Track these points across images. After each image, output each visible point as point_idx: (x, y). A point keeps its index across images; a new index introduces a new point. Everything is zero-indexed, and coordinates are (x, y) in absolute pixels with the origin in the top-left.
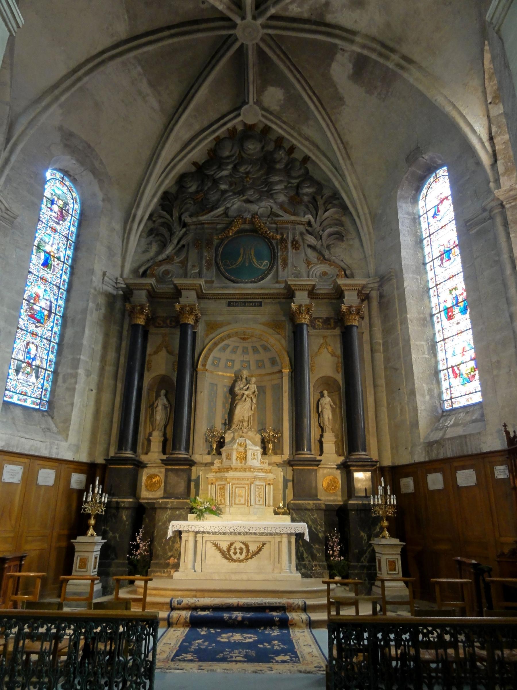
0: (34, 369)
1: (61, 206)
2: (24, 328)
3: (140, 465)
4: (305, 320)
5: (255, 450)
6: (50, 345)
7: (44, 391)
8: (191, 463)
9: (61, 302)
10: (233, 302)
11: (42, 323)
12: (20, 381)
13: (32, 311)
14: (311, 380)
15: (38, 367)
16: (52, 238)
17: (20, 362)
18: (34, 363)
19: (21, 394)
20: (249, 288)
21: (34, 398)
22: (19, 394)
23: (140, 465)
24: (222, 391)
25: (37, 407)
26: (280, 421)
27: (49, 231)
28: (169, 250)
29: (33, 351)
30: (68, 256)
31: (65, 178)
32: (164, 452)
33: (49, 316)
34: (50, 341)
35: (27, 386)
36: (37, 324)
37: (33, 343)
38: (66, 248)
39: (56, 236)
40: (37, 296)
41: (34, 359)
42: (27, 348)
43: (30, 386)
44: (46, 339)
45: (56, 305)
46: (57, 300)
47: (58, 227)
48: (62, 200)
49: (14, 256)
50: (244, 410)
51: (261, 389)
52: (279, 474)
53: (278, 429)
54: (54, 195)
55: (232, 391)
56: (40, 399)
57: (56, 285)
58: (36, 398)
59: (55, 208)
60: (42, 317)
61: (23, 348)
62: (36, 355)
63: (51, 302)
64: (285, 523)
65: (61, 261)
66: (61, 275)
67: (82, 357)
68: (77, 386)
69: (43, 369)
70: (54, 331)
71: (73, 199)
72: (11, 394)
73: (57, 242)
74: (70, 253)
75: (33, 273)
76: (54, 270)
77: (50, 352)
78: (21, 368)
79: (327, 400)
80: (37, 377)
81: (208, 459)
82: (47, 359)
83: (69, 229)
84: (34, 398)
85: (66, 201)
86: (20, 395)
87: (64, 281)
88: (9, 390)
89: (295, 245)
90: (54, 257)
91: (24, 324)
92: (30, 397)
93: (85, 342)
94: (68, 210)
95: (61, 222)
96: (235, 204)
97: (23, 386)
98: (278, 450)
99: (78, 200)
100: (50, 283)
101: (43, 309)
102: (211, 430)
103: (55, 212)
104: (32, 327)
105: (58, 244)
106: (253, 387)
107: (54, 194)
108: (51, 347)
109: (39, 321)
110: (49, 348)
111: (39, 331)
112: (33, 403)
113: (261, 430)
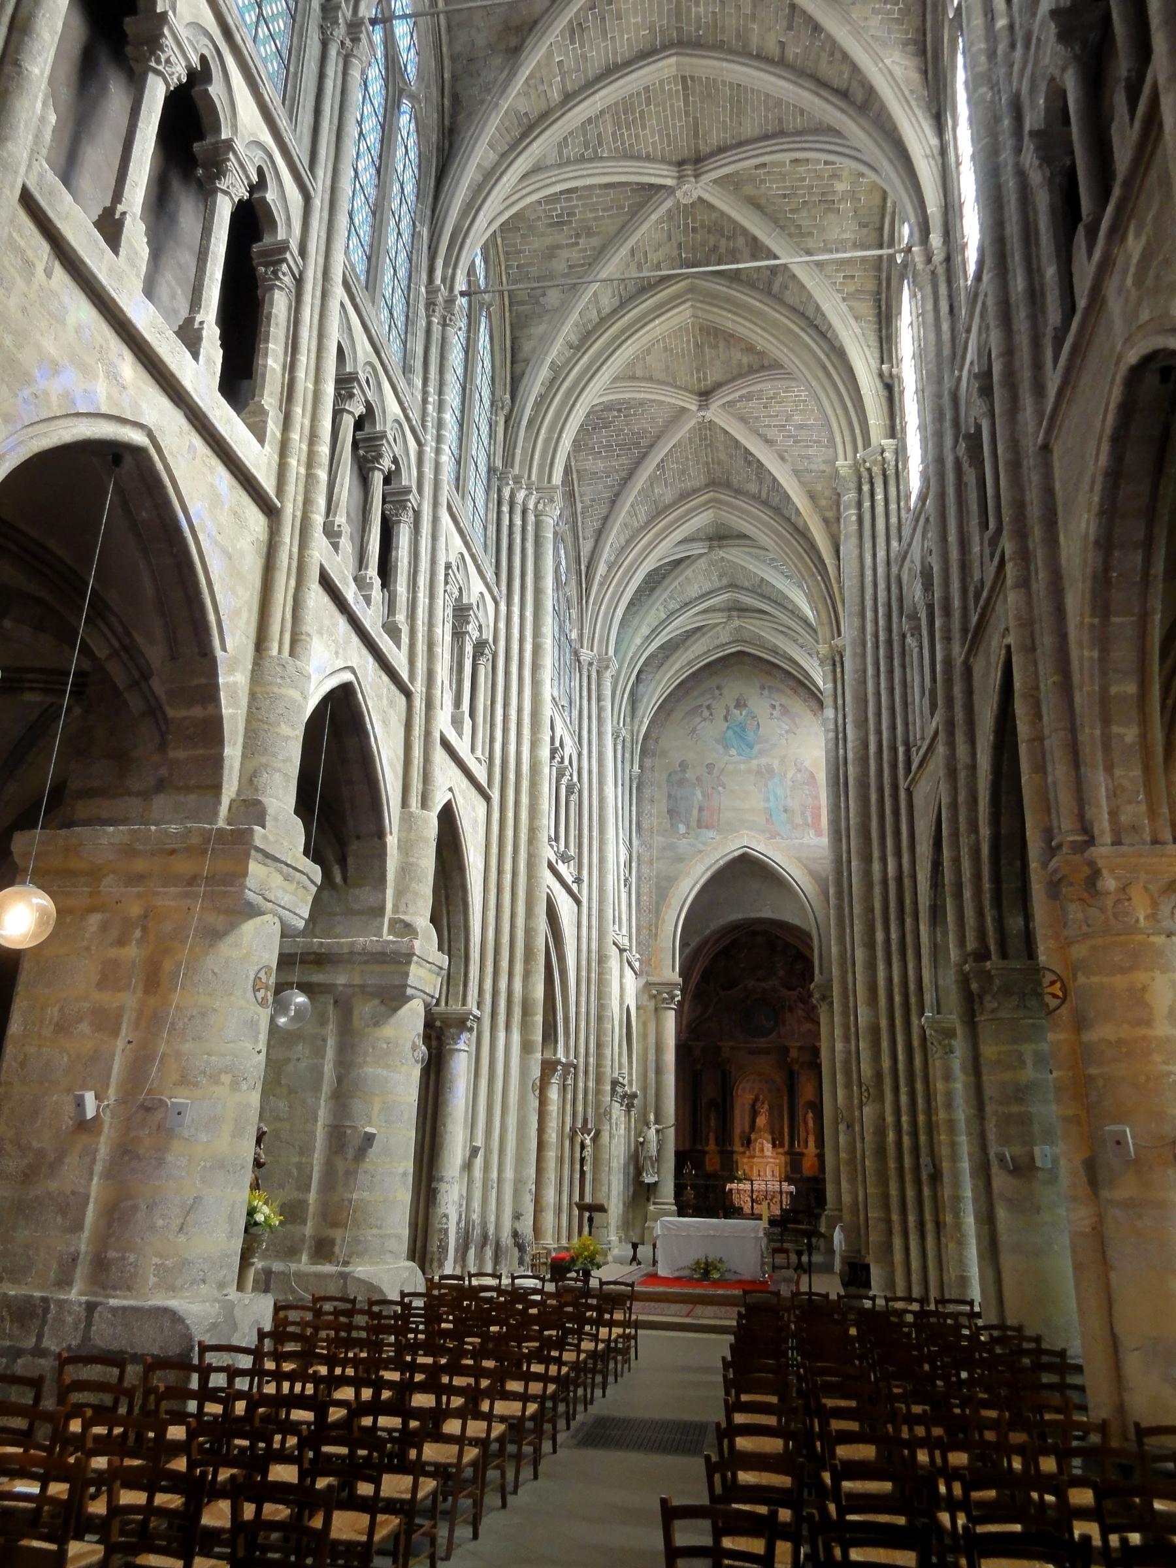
3: (704, 1153)
4: (796, 1067)
5: (768, 1146)
8: (732, 1152)
10: (752, 1052)
14: (801, 1102)
20: (762, 1042)
23: (704, 1153)
24: (747, 1107)
26: (782, 1128)
28: (710, 1011)
32: (717, 1144)
50: (761, 1121)
51: (771, 1108)
52: (782, 1159)
53: (782, 1133)
55: (753, 1106)
64: (786, 1187)
79: (810, 1115)
81: (741, 1149)
89: (791, 1009)
96: (751, 983)
98: (782, 1145)
102: (743, 1132)
106: (766, 1106)
113: (772, 1132)
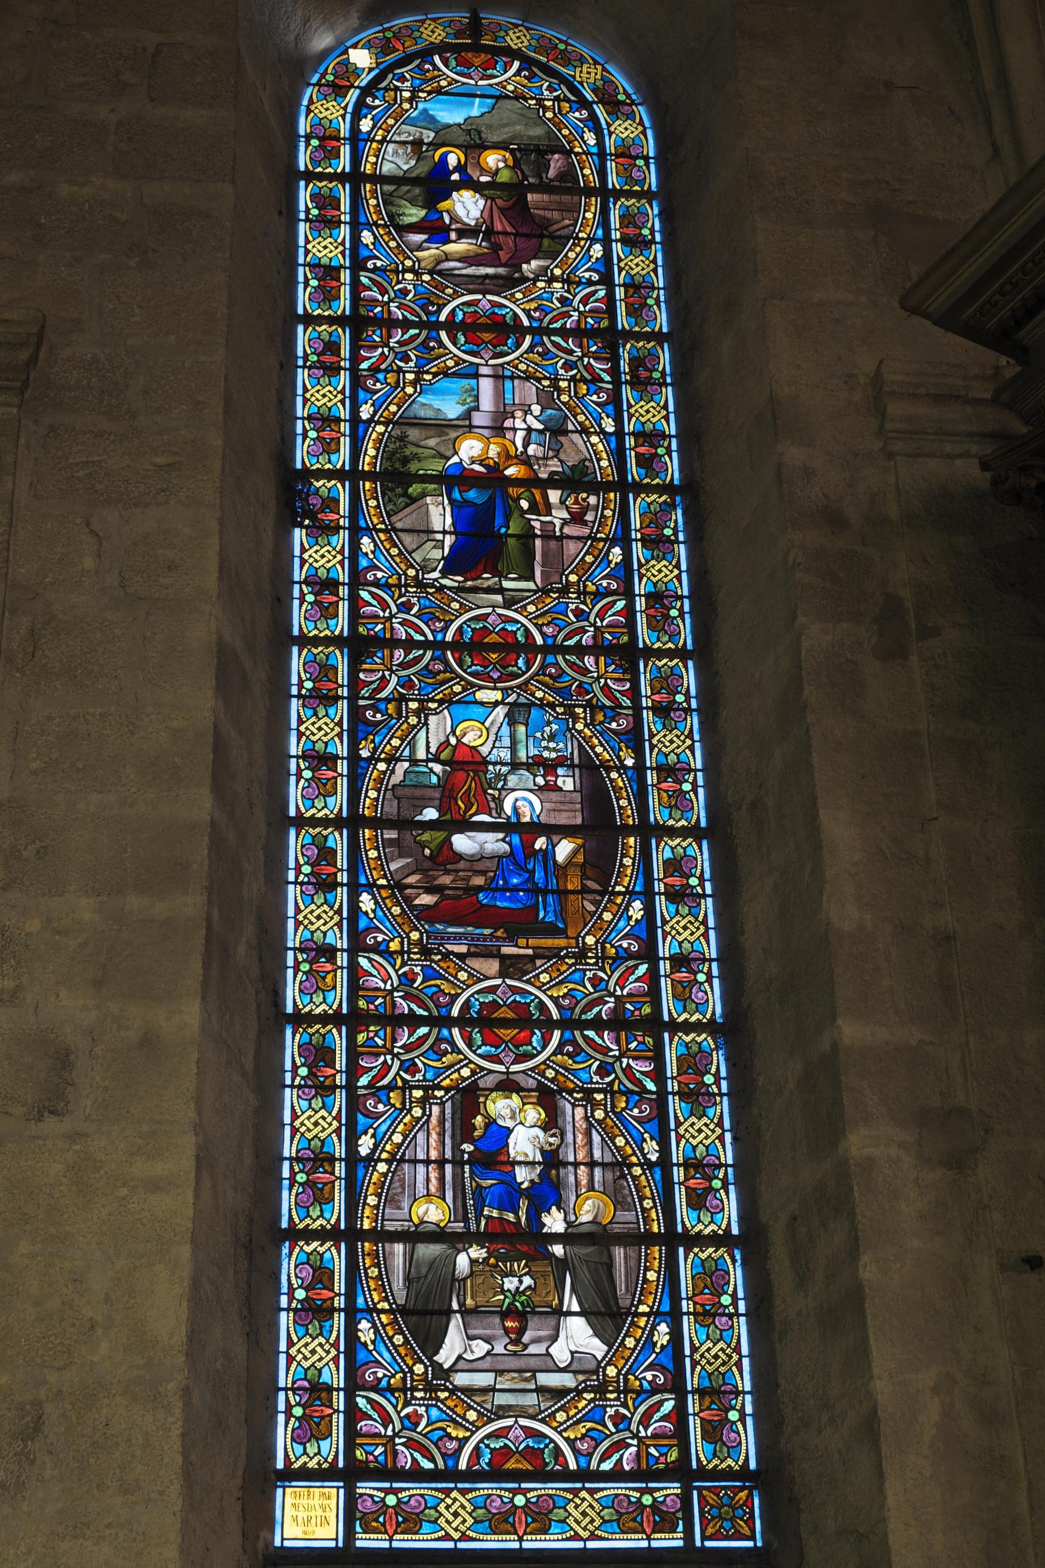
0: (563, 1265)
1: (504, 177)
2: (404, 1006)
6: (658, 1057)
7: (692, 1404)
9: (680, 742)
11: (551, 930)
12: (461, 1379)
13: (446, 880)
15: (594, 1238)
16: (486, 386)
17: (427, 1251)
18: (554, 1222)
19: (495, 1474)
21: (617, 1475)
22: (472, 1475)
25: (673, 1541)
27: (454, 350)
29: (525, 1141)
30: (650, 437)
31: (488, 17)
33: (598, 864)
34: (656, 1025)
35: (531, 1399)
36: (507, 950)
37: (508, 1086)
38: (615, 399)
39: (519, 354)
40: (465, 763)
41: (548, 1192)
42: (464, 1131)
43: (559, 1393)
44: (618, 1023)
45: (640, 768)
46: (634, 738)
47: (514, 306)
48: (496, 146)
49: (89, 563)
54: (435, 145)
56: (682, 1471)
57: (598, 649)
58: (643, 1474)
59: (467, 206)
60: (536, 891)
61: (428, 1145)
62: (551, 1160)
63: (590, 769)
65: (595, 487)
66: (626, 572)
67: (850, 1031)
68: (868, 1270)
69: (649, 1239)
70: (665, 949)
71: (583, 103)
72: (412, 1489)
73: (530, 390)
74: (656, 411)
75: (394, 643)
76: (555, 563)
77: (674, 1105)
78: (453, 1282)
80: (607, 1316)
82: (665, 1162)
83: (607, 280)
84: (617, 1475)
85: (538, 131)
86: (486, 1487)
87: (656, 598)
88: (389, 1473)
90: (532, 482)
91: (408, 979)
92: (584, 1475)
93: (844, 911)
94: (568, 175)
95: (532, 267)
97: (503, 1411)
99: (622, 82)
100: (546, 649)
101: (537, 828)
103: (465, 232)
104: (477, 983)
105: (546, 400)
107: (429, 136)
108: (671, 1068)
109: (521, 924)
110: (658, 1075)
111: (542, 991)
112: (627, 1516)
